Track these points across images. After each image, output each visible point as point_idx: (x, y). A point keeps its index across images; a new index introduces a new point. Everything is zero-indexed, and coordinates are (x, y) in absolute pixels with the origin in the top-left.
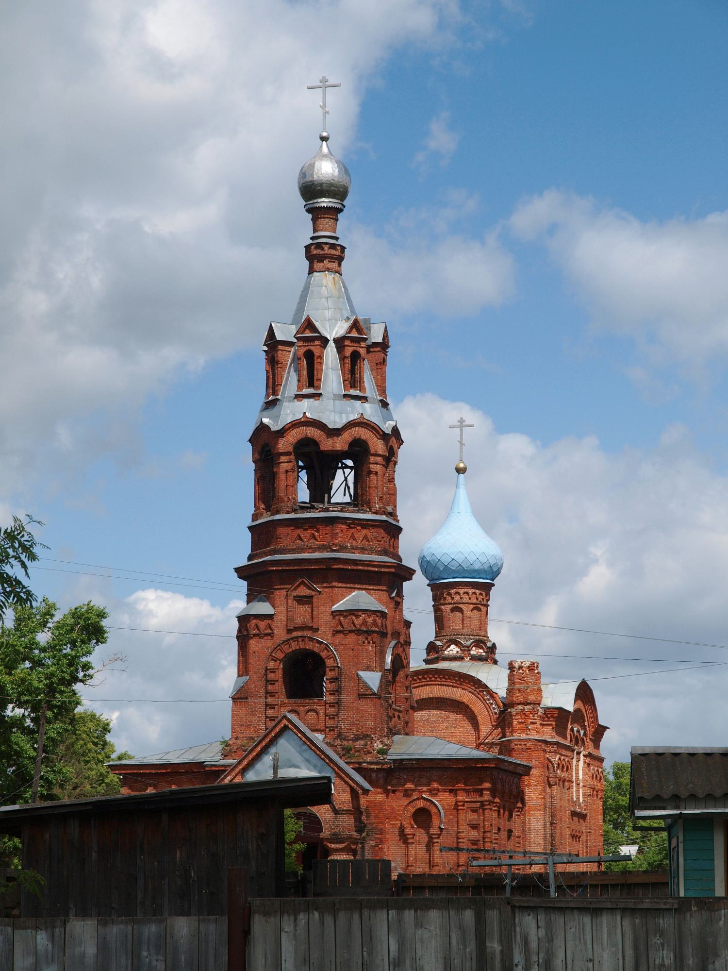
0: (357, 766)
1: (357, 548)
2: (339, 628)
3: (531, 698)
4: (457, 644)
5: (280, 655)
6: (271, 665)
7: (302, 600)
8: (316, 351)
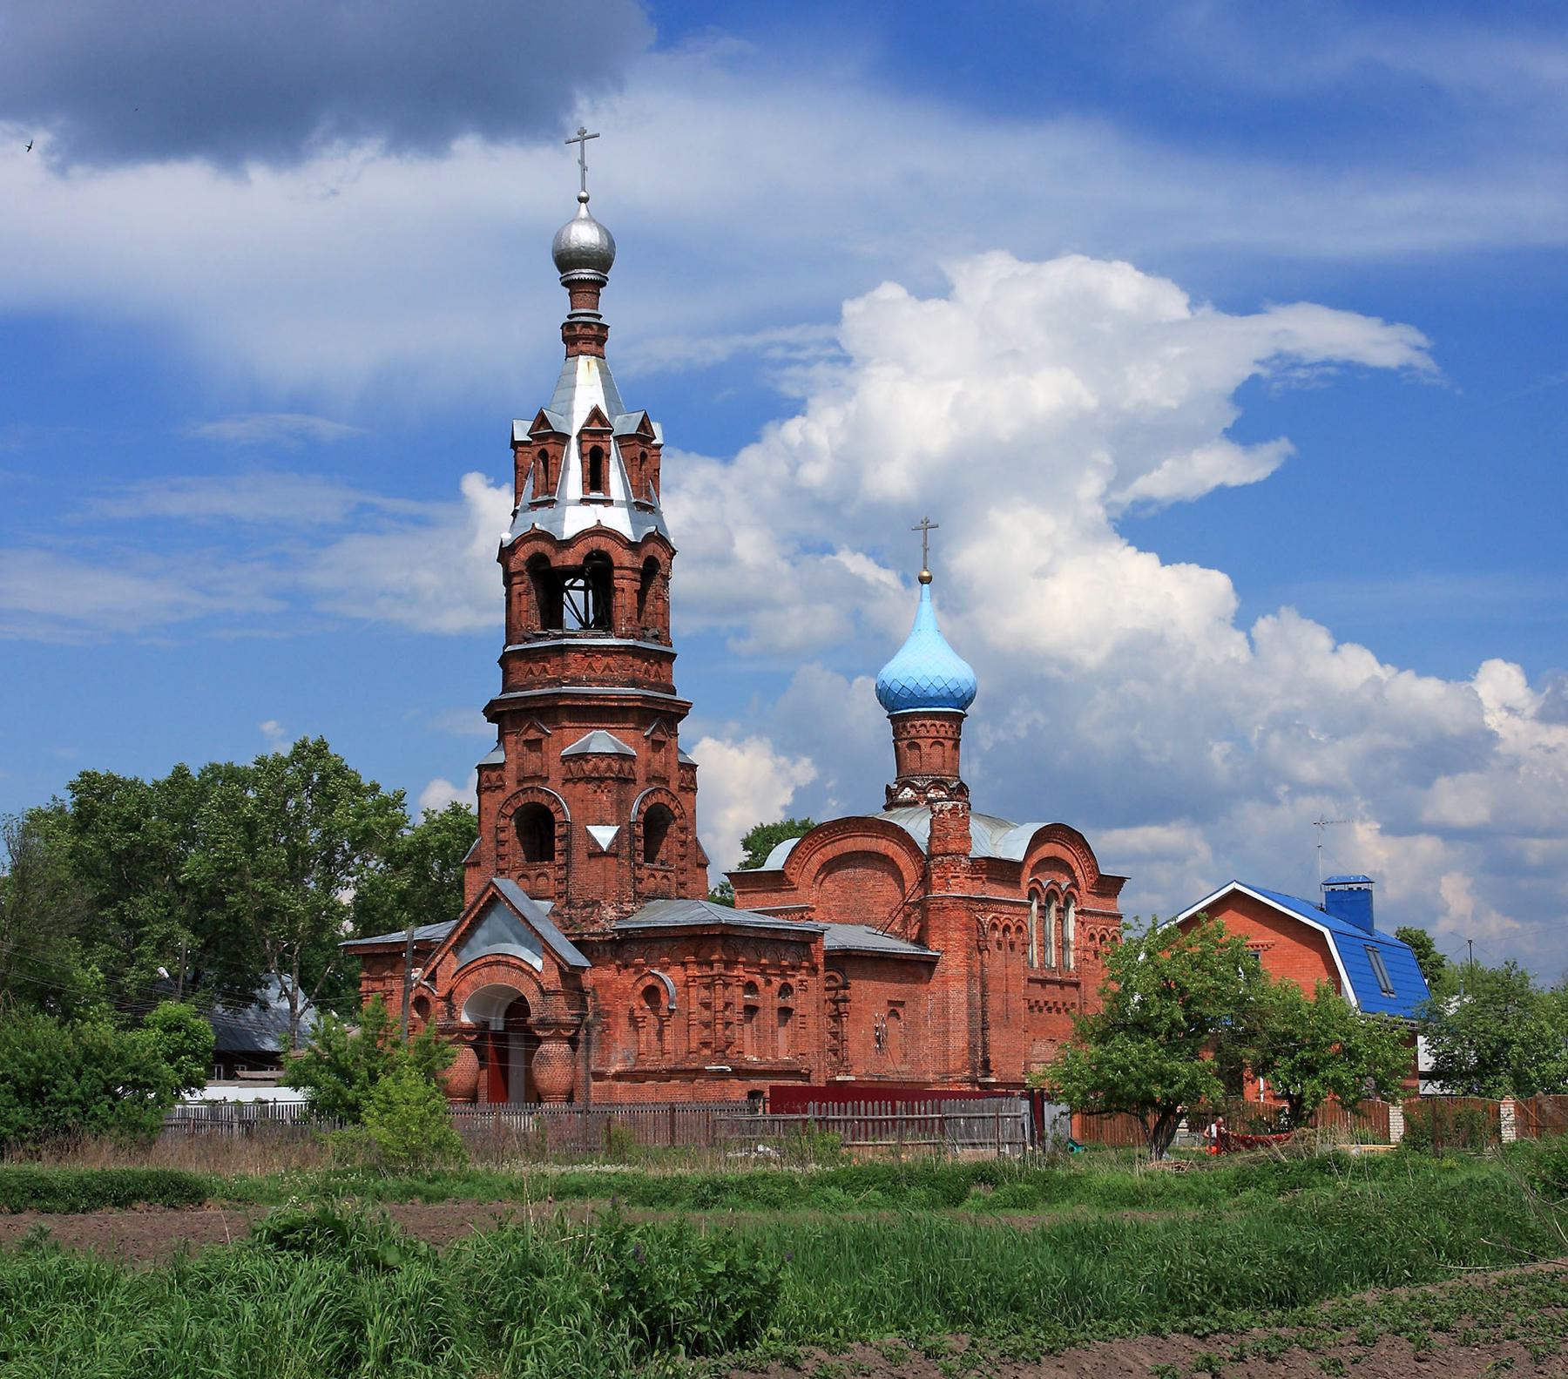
0: (578, 938)
1: (595, 680)
2: (569, 776)
3: (952, 847)
4: (913, 787)
5: (510, 811)
6: (502, 822)
7: (534, 745)
8: (551, 450)
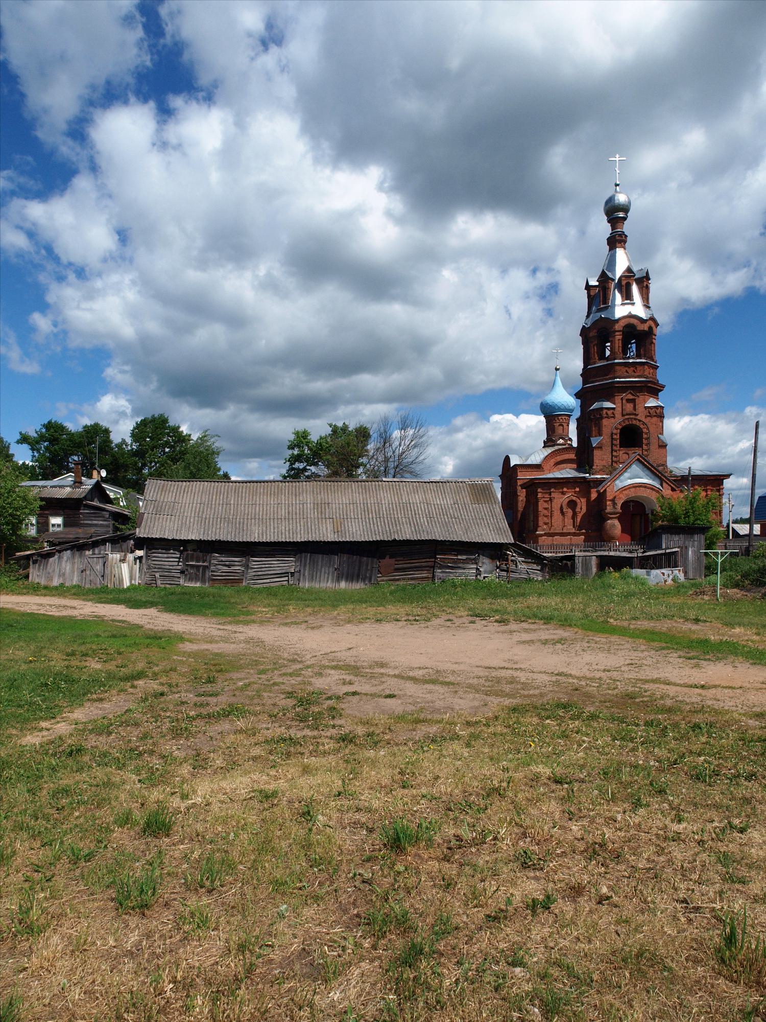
6: (615, 431)
